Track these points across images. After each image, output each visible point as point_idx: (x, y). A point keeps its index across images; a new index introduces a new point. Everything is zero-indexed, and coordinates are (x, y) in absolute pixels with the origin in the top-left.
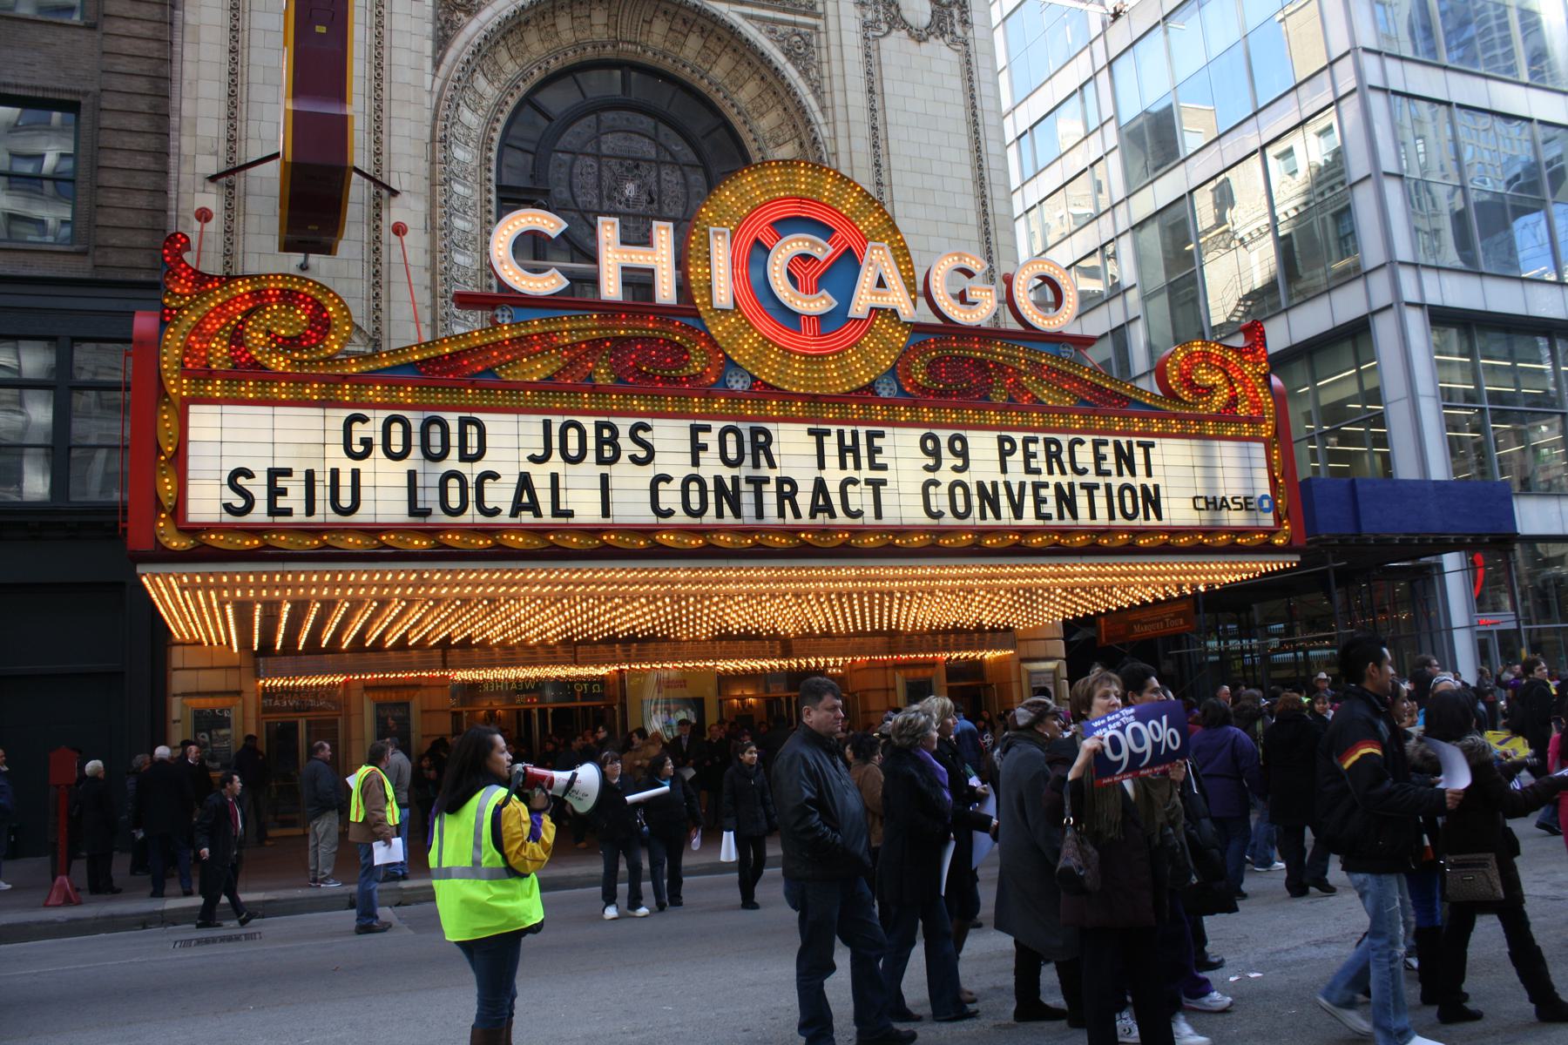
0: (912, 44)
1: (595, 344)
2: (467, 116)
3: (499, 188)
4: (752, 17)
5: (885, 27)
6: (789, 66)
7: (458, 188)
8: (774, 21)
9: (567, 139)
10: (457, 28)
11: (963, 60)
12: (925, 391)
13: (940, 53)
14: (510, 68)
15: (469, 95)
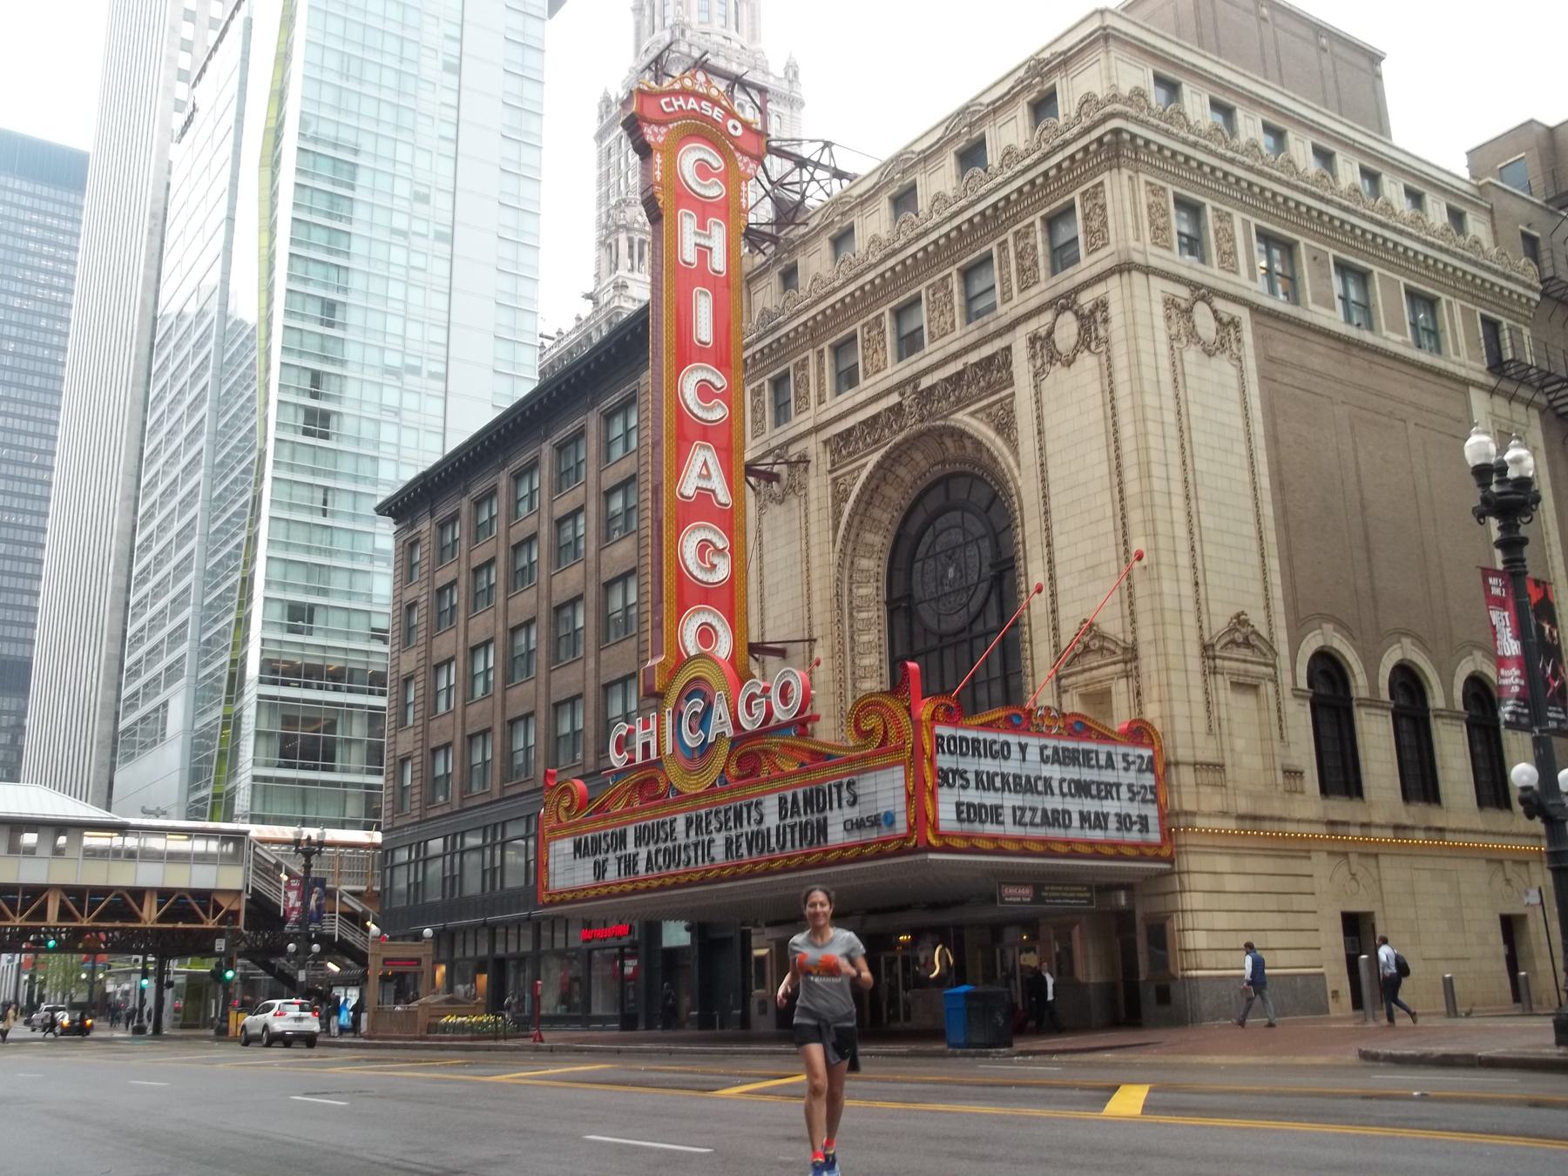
0: (1065, 370)
1: (635, 786)
2: (865, 563)
3: (887, 603)
4: (976, 412)
5: (1047, 367)
6: (999, 442)
7: (864, 615)
8: (990, 406)
9: (922, 549)
10: (840, 513)
11: (1104, 358)
12: (739, 778)
13: (1087, 362)
14: (886, 517)
15: (861, 550)
